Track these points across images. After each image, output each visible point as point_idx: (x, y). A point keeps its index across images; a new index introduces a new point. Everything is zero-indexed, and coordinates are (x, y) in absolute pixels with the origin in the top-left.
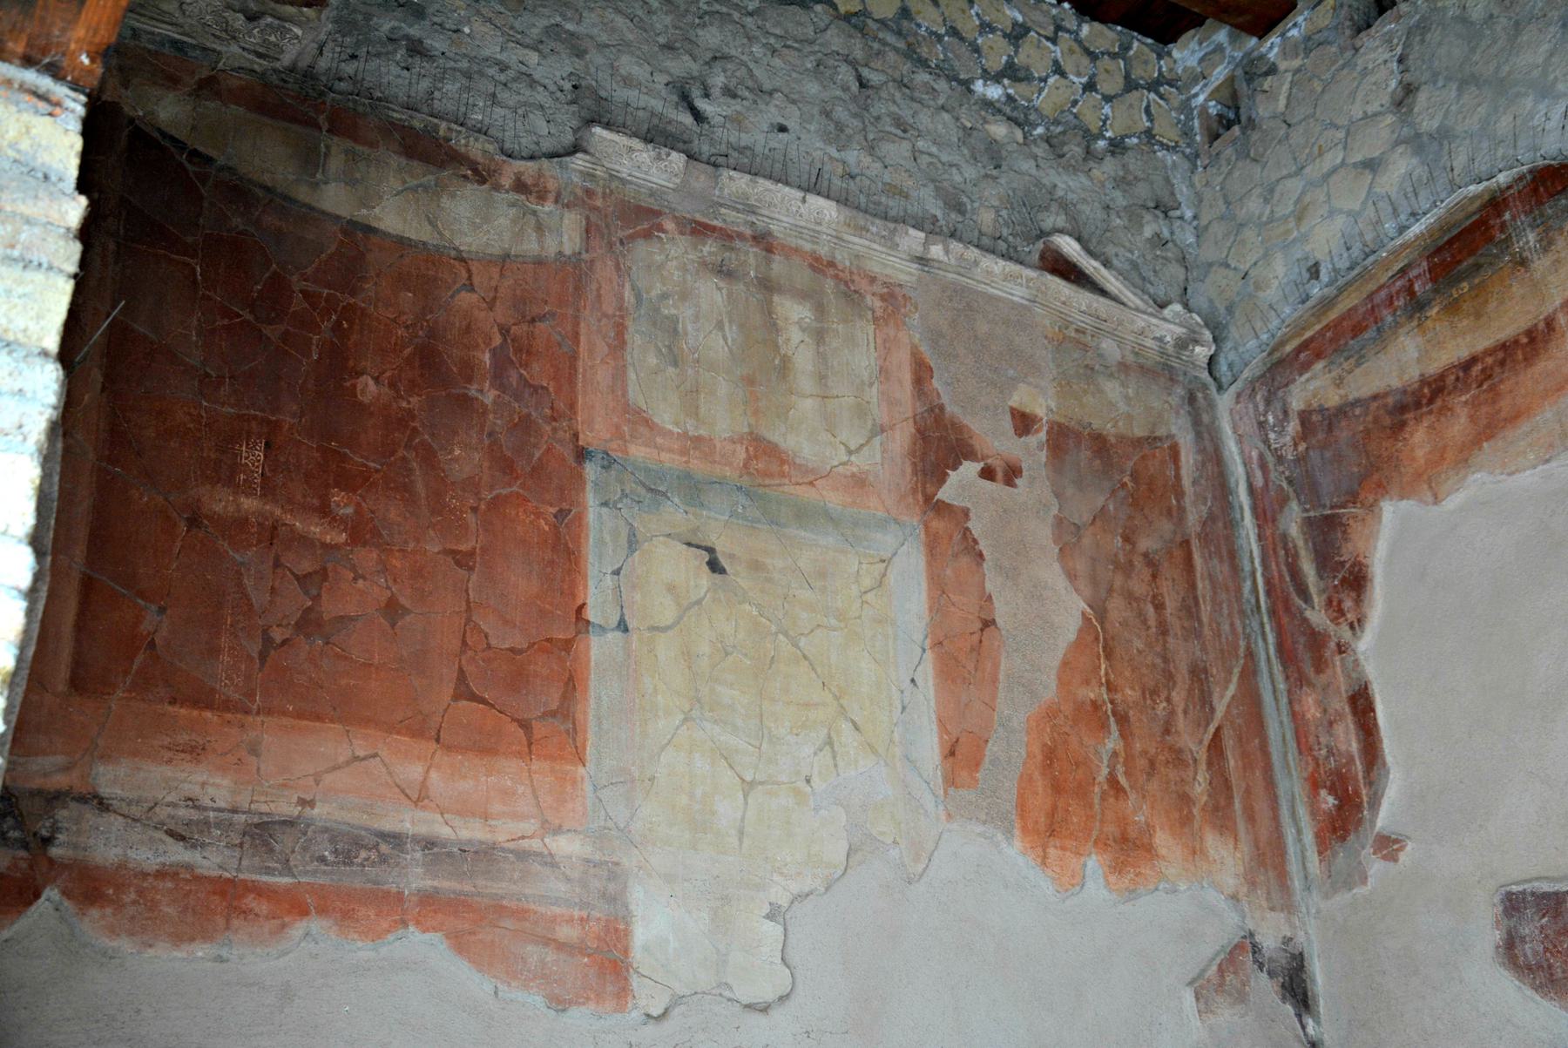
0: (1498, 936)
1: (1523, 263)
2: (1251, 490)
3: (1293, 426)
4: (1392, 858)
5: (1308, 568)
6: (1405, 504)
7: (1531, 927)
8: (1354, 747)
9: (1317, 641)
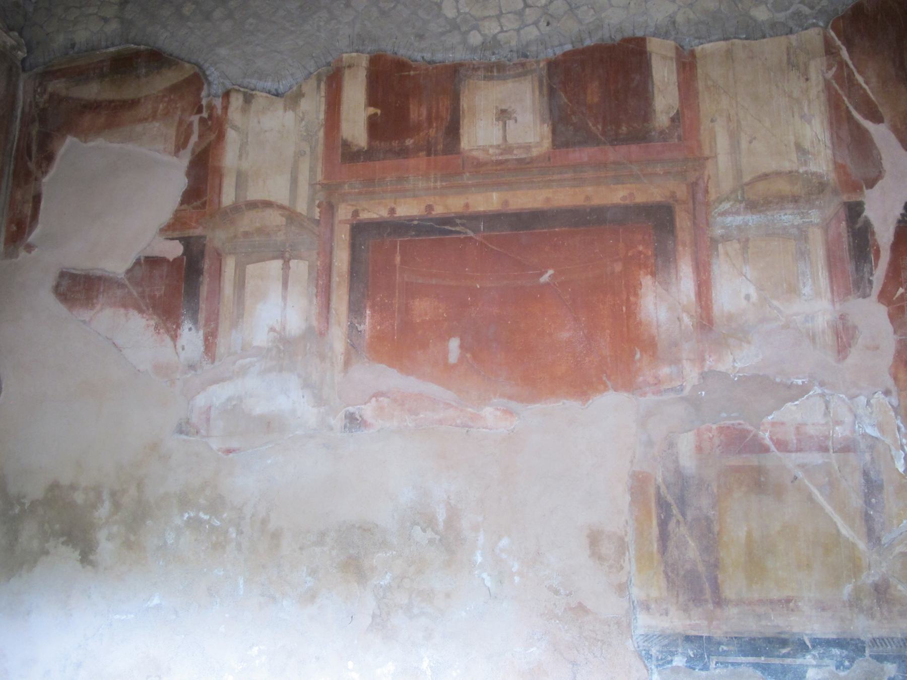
0: (54, 283)
1: (138, 77)
2: (23, 112)
3: (46, 97)
4: (29, 252)
5: (34, 148)
6: (75, 139)
7: (65, 282)
8: (29, 213)
9: (28, 174)
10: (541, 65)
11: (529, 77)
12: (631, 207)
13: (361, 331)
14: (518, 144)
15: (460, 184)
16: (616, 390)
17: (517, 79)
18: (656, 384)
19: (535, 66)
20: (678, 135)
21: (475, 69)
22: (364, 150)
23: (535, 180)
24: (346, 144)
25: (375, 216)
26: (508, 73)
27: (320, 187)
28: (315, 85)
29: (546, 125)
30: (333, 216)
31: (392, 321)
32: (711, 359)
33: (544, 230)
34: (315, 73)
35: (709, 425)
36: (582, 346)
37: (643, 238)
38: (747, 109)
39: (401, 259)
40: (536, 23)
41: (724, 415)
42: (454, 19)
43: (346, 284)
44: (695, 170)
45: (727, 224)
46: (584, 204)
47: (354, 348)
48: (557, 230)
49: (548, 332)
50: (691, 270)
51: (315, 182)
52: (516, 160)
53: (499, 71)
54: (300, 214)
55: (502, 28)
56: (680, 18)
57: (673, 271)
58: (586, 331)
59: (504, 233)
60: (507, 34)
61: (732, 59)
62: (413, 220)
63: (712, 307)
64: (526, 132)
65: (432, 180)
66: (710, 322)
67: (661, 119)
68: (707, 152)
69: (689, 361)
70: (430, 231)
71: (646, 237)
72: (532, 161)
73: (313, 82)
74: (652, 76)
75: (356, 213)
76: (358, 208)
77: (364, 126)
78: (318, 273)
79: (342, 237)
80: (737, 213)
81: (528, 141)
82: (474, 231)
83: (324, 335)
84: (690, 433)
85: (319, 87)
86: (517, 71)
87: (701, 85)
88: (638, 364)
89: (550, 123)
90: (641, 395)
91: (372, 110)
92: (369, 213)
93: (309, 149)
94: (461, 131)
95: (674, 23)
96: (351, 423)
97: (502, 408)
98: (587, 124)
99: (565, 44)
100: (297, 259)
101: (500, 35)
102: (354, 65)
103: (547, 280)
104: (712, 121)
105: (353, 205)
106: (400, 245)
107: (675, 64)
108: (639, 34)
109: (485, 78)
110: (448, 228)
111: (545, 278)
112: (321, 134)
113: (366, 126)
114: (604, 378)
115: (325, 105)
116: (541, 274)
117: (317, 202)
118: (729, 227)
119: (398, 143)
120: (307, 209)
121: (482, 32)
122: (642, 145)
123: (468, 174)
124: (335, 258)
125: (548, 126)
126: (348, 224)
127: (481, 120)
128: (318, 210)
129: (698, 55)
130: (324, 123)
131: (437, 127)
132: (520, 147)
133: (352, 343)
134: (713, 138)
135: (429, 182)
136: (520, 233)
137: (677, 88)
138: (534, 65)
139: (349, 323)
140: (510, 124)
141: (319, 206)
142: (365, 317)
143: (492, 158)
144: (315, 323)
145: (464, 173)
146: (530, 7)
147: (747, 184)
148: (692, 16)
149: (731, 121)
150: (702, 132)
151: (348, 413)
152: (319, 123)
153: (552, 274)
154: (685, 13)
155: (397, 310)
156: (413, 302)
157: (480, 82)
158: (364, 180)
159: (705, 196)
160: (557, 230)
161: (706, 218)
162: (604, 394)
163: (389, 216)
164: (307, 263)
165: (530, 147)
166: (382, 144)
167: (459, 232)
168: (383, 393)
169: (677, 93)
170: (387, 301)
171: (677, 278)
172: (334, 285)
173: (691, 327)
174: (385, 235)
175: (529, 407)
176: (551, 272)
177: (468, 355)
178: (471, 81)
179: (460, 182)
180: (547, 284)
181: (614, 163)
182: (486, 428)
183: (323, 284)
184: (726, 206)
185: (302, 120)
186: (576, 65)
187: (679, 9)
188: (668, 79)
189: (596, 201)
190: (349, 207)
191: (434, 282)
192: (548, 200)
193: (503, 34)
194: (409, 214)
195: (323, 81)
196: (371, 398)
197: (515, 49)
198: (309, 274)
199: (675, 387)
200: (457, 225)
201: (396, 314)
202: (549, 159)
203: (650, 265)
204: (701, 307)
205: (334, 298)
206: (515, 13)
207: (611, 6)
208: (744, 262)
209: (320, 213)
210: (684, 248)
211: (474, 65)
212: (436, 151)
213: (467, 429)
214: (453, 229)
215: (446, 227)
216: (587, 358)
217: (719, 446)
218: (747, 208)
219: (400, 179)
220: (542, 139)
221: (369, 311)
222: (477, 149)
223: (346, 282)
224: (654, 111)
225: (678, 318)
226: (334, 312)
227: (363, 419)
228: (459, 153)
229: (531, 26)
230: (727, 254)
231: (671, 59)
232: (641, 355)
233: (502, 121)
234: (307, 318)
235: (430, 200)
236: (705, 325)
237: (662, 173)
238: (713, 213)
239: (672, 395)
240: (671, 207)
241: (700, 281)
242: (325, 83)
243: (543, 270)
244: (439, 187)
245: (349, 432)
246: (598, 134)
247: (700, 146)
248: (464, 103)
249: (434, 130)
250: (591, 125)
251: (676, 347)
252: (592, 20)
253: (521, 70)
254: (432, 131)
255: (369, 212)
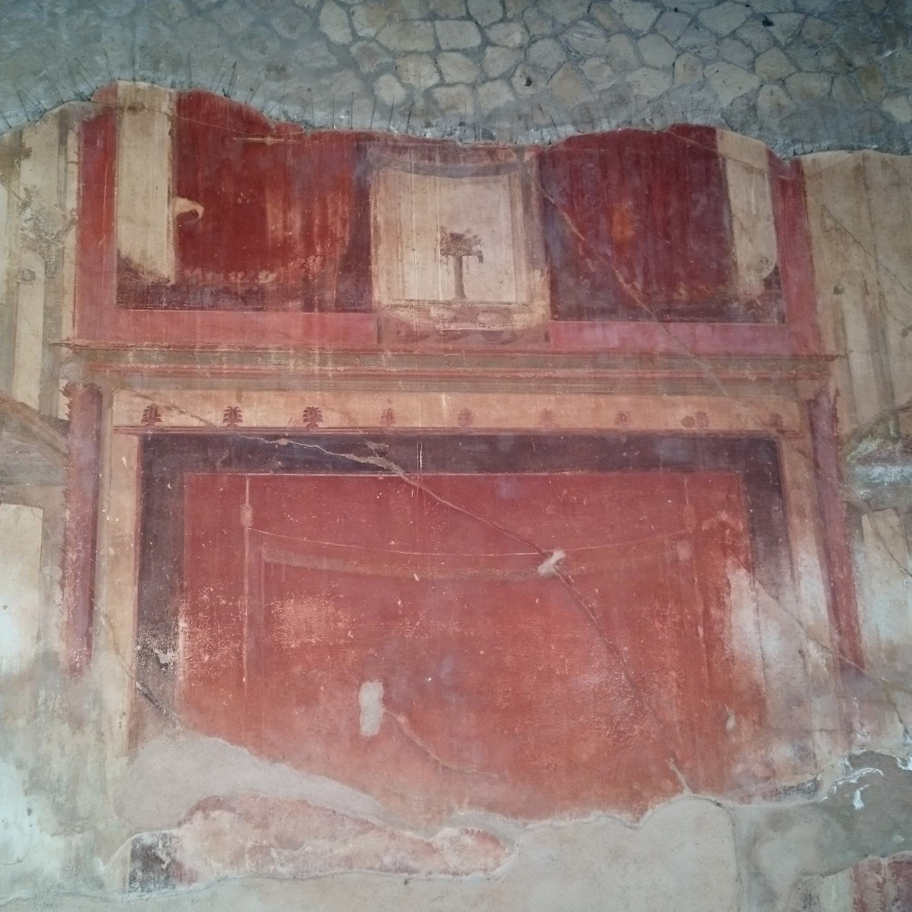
10: (527, 157)
11: (504, 178)
12: (701, 439)
13: (166, 665)
14: (486, 303)
15: (374, 371)
16: (695, 790)
17: (480, 178)
18: (767, 778)
19: (514, 159)
20: (779, 313)
21: (398, 148)
22: (169, 285)
23: (520, 375)
24: (127, 268)
25: (196, 423)
26: (462, 164)
27: (71, 351)
28: (55, 132)
29: (537, 273)
30: (100, 417)
31: (237, 645)
32: (864, 730)
33: (544, 474)
34: (56, 110)
35: (875, 858)
36: (625, 701)
37: (728, 498)
38: (895, 276)
39: (255, 517)
40: (507, 77)
41: (899, 838)
42: (346, 47)
43: (132, 564)
44: (812, 378)
45: (874, 479)
46: (616, 427)
47: (152, 702)
48: (567, 473)
49: (558, 673)
50: (817, 562)
51: (57, 341)
52: (483, 332)
53: (444, 159)
54: (24, 405)
55: (442, 78)
56: (764, 102)
57: (785, 562)
58: (632, 673)
59: (466, 474)
60: (453, 91)
61: (865, 184)
62: (277, 437)
63: (859, 632)
64: (502, 282)
65: (317, 358)
66: (859, 660)
67: (747, 280)
68: (830, 348)
69: (824, 733)
70: (314, 462)
71: (733, 496)
72: (514, 336)
73: (50, 129)
74: (728, 200)
75: (152, 414)
76: (157, 403)
77: (168, 235)
78: (65, 535)
79: (122, 462)
80: (890, 460)
81: (506, 299)
82: (404, 467)
83: (80, 671)
84: (841, 876)
85: (63, 141)
86: (481, 164)
87: (814, 226)
88: (734, 740)
89: (546, 270)
90: (742, 800)
91: (184, 205)
92: (183, 416)
93: (42, 269)
94: (373, 267)
95: (754, 108)
96: (146, 868)
97: (476, 830)
98: (615, 278)
99: (563, 124)
100: (16, 503)
101: (439, 89)
102: (143, 107)
103: (553, 570)
104: (837, 291)
105: (145, 397)
106: (251, 486)
107: (767, 183)
108: (698, 121)
109: (417, 170)
110: (350, 456)
111: (547, 567)
112: (71, 240)
113: (172, 235)
114: (672, 767)
115: (79, 181)
116: (543, 557)
117: (63, 383)
118: (878, 484)
119: (242, 279)
120: (40, 397)
121: (404, 81)
122: (717, 324)
123: (389, 353)
124: (106, 505)
125: (542, 275)
126: (135, 434)
127: (414, 250)
128: (64, 401)
129: (806, 171)
130: (77, 217)
131: (323, 255)
132: (490, 310)
133: (146, 691)
134: (840, 323)
135: (310, 364)
136: (496, 477)
137: (773, 228)
138: (512, 156)
139: (139, 647)
140: (470, 262)
141: (67, 392)
142: (176, 634)
143: (437, 326)
144: (58, 646)
145: (382, 351)
146: (494, 45)
147: (904, 409)
148: (784, 101)
149: (868, 294)
150: (819, 308)
151: (138, 846)
152: (65, 217)
153: (560, 560)
154: (772, 93)
155: (246, 621)
156: (282, 606)
157: (409, 175)
158: (169, 347)
159: (832, 427)
160: (567, 473)
161: (837, 466)
162: (673, 799)
163: (226, 424)
164: (40, 512)
165: (509, 310)
166: (209, 276)
167: (375, 468)
168: (218, 800)
169: (773, 236)
170: (224, 602)
171: (792, 576)
172: (104, 564)
173: (825, 669)
174: (218, 464)
175: (530, 826)
176: (558, 555)
177: (402, 719)
178: (391, 172)
179: (373, 367)
180: (553, 578)
181: (668, 354)
182: (446, 872)
183: (78, 558)
184: (870, 446)
185: (25, 205)
186: (592, 165)
187: (761, 86)
188: (758, 210)
189: (637, 424)
190: (137, 400)
191: (325, 565)
192: (547, 415)
193: (444, 90)
194: (269, 425)
195: (72, 129)
196: (192, 813)
197: (468, 121)
198: (46, 536)
199: (803, 784)
200: (369, 453)
201: (245, 630)
202: (547, 338)
203: (743, 549)
204: (840, 632)
205: (104, 590)
206: (465, 52)
207: (643, 64)
208: (909, 551)
209: (70, 407)
210: (801, 521)
211: (395, 141)
212: (321, 301)
213: (406, 875)
214: (362, 460)
215: (347, 456)
216: (635, 727)
217: (896, 900)
218: (907, 452)
219: (249, 352)
220: (532, 297)
221: (185, 621)
222: (406, 307)
223: (132, 557)
224: (735, 263)
225: (800, 652)
226: (104, 623)
227: (173, 861)
228: (370, 310)
229: (498, 82)
230: (878, 535)
231: (761, 173)
232: (738, 722)
233: (454, 255)
234: (39, 632)
235: (314, 399)
236: (849, 665)
237: (754, 379)
238: (848, 458)
239: (800, 800)
240: (774, 443)
241: (833, 582)
242: (78, 134)
243: (544, 551)
244: (330, 375)
245: (142, 891)
246: (635, 296)
247: (818, 336)
248: (378, 214)
249: (318, 260)
250: (621, 280)
251: (799, 705)
252: (608, 85)
253: (487, 162)
254: (315, 260)
255: (182, 412)
